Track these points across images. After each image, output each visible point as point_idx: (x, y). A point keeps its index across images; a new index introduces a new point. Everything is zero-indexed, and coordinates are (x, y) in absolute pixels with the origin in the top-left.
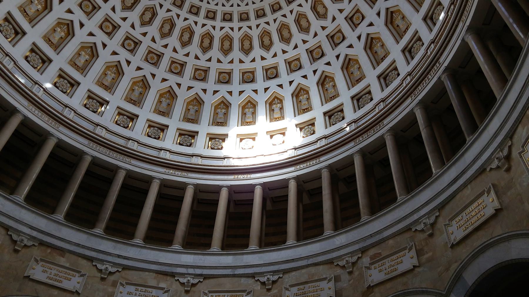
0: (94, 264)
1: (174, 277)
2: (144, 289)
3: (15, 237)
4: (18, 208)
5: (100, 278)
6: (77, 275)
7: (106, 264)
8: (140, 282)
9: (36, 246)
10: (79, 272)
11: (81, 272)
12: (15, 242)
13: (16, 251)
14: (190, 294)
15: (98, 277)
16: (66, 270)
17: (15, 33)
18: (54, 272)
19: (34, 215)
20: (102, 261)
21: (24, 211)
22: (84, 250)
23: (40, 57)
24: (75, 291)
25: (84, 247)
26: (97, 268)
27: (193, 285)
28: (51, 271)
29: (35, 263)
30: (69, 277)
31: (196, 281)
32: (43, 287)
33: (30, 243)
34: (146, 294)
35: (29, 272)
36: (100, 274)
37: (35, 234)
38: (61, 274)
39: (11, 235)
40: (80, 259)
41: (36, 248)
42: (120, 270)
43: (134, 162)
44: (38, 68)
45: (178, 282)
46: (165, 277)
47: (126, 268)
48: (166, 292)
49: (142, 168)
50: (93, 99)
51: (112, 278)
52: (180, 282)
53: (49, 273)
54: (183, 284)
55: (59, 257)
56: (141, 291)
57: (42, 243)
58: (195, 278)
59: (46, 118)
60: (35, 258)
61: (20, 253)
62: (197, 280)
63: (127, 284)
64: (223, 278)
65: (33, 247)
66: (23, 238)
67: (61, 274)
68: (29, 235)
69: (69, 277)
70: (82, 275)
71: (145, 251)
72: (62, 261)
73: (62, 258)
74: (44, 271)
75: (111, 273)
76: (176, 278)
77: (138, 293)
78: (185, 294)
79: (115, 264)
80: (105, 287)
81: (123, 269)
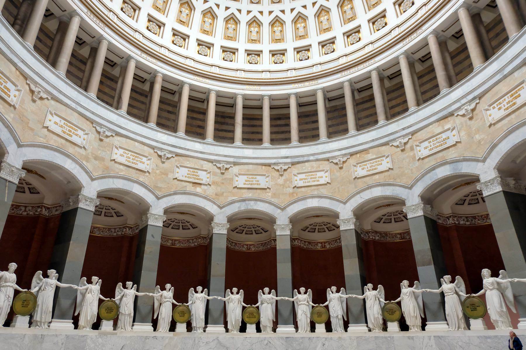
0: (390, 145)
1: (453, 115)
2: (434, 138)
3: (335, 161)
4: (326, 145)
5: (401, 151)
6: (384, 158)
7: (398, 140)
8: (429, 136)
9: (349, 158)
10: (384, 156)
11: (385, 155)
12: (337, 164)
13: (341, 168)
14: (474, 119)
15: (399, 151)
16: (375, 160)
17: (258, 56)
18: (368, 166)
19: (337, 142)
20: (394, 140)
21: (330, 144)
22: (379, 141)
23: (280, 54)
24: (388, 169)
25: (377, 139)
26: (394, 146)
27: (473, 110)
28: (367, 166)
29: (355, 167)
30: (380, 163)
31: (473, 105)
32: (368, 178)
33: (345, 159)
34: (438, 140)
35: (356, 175)
36: (399, 149)
37: (344, 152)
38: (374, 164)
39: (332, 162)
40: (380, 148)
41: (351, 159)
42: (410, 137)
43: (377, 59)
44: (284, 60)
45: (459, 116)
46: (446, 120)
47: (413, 133)
48: (452, 130)
49: (385, 58)
50: (326, 45)
51: (408, 146)
52: (461, 116)
53: (366, 168)
54: (463, 115)
55: (366, 155)
56: (433, 141)
57: (352, 155)
58: (471, 104)
59: (307, 84)
60: (353, 165)
61: (343, 167)
62: (473, 104)
63: (421, 143)
64: (496, 86)
65: (348, 160)
66: (339, 159)
67: (374, 164)
68: (341, 155)
69: (380, 163)
70: (387, 157)
71: (420, 113)
72: (370, 156)
73: (369, 155)
74: (363, 169)
75: (405, 144)
76: (456, 115)
77: (431, 144)
78: (470, 121)
79: (404, 136)
80: (407, 154)
81: (412, 135)
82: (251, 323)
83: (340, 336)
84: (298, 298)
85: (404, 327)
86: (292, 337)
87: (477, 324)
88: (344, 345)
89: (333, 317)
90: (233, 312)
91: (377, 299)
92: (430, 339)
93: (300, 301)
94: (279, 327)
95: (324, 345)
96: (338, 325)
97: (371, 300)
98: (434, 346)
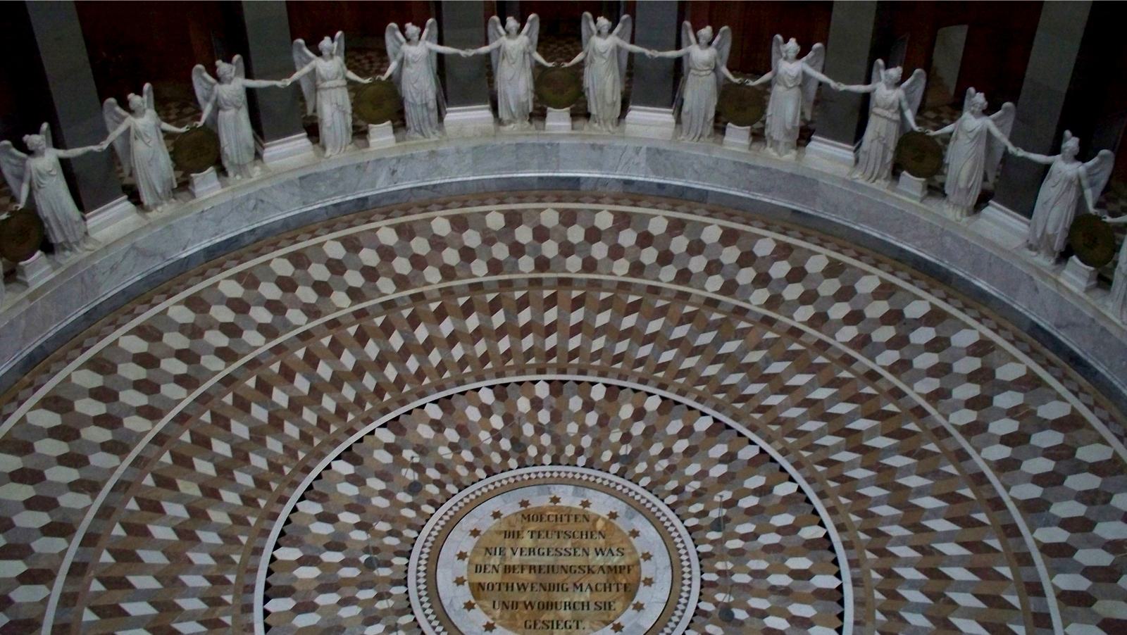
82: (201, 170)
83: (434, 149)
84: (314, 71)
85: (581, 113)
86: (316, 174)
87: (737, 137)
88: (443, 165)
89: (414, 105)
90: (150, 165)
91: (527, 56)
92: (637, 153)
93: (323, 80)
94: (268, 146)
95: (394, 172)
96: (427, 123)
97: (514, 63)
98: (643, 165)
